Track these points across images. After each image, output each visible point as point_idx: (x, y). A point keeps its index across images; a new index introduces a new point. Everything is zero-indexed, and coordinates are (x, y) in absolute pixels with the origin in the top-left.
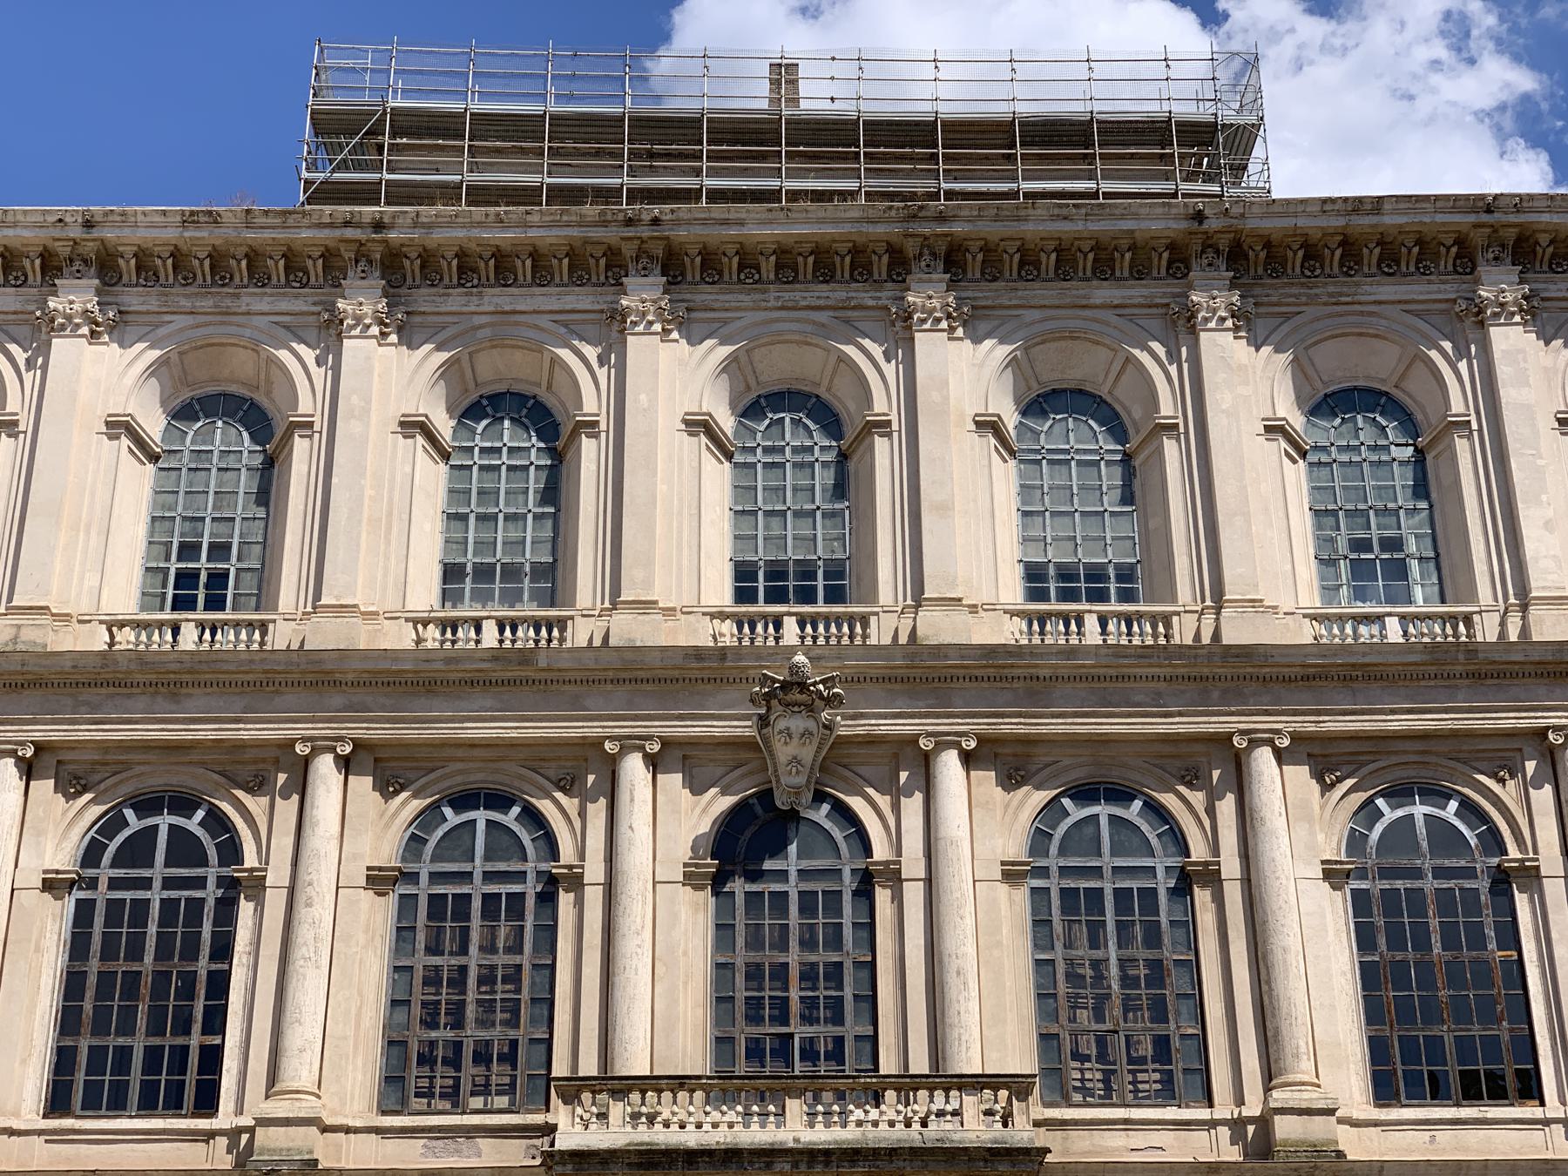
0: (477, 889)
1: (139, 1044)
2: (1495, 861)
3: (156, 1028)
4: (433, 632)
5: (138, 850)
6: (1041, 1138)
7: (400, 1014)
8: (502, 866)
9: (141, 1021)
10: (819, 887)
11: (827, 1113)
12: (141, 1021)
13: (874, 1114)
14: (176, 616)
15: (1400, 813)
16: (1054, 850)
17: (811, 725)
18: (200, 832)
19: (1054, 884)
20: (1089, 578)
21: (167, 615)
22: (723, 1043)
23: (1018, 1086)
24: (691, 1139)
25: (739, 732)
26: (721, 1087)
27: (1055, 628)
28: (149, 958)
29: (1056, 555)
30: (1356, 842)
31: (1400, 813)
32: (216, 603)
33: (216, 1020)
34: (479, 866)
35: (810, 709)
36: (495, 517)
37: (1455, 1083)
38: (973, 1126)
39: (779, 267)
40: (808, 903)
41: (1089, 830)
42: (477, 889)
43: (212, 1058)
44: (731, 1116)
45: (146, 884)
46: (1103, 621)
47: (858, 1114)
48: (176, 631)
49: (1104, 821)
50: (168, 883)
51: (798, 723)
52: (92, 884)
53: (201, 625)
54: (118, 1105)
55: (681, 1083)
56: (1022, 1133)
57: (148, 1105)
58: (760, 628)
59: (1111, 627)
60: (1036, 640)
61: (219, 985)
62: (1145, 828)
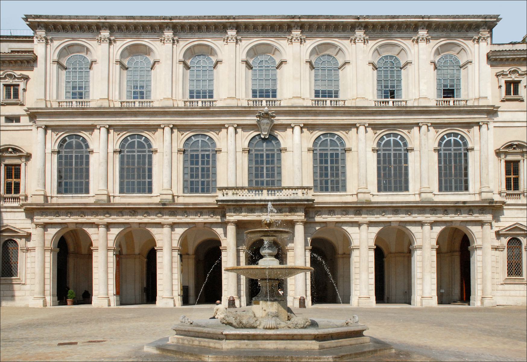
0: (200, 154)
1: (136, 181)
2: (405, 148)
3: (139, 177)
4: (188, 104)
5: (132, 145)
6: (313, 198)
7: (186, 176)
8: (205, 149)
9: (136, 176)
10: (270, 153)
11: (271, 194)
12: (136, 176)
13: (281, 194)
14: (134, 100)
15: (388, 139)
16: (318, 145)
17: (268, 121)
18: (143, 142)
19: (318, 152)
20: (328, 93)
21: (132, 100)
22: (250, 181)
23: (309, 188)
24: (245, 198)
25: (253, 123)
26: (250, 189)
27: (321, 104)
28: (136, 165)
29: (321, 88)
30: (379, 144)
31: (388, 139)
32: (143, 98)
33: (150, 177)
34: (200, 149)
35: (268, 118)
36: (194, 80)
37: (393, 188)
38: (300, 195)
39: (262, 28)
40: (268, 156)
41: (326, 142)
42: (200, 154)
43: (150, 184)
44: (253, 194)
45: (134, 152)
46: (331, 101)
47: (278, 194)
48: (134, 102)
49: (329, 140)
50: (138, 152)
51: (265, 121)
52: (124, 151)
53: (139, 102)
54: (133, 192)
55: (242, 188)
56: (310, 197)
57: (139, 192)
58: (258, 103)
59: (332, 103)
60: (317, 105)
61: (150, 170)
62: (337, 142)
